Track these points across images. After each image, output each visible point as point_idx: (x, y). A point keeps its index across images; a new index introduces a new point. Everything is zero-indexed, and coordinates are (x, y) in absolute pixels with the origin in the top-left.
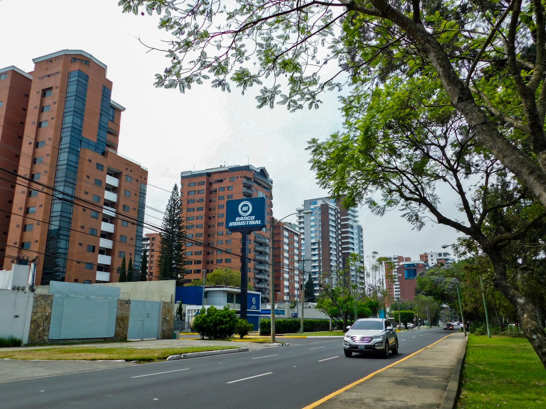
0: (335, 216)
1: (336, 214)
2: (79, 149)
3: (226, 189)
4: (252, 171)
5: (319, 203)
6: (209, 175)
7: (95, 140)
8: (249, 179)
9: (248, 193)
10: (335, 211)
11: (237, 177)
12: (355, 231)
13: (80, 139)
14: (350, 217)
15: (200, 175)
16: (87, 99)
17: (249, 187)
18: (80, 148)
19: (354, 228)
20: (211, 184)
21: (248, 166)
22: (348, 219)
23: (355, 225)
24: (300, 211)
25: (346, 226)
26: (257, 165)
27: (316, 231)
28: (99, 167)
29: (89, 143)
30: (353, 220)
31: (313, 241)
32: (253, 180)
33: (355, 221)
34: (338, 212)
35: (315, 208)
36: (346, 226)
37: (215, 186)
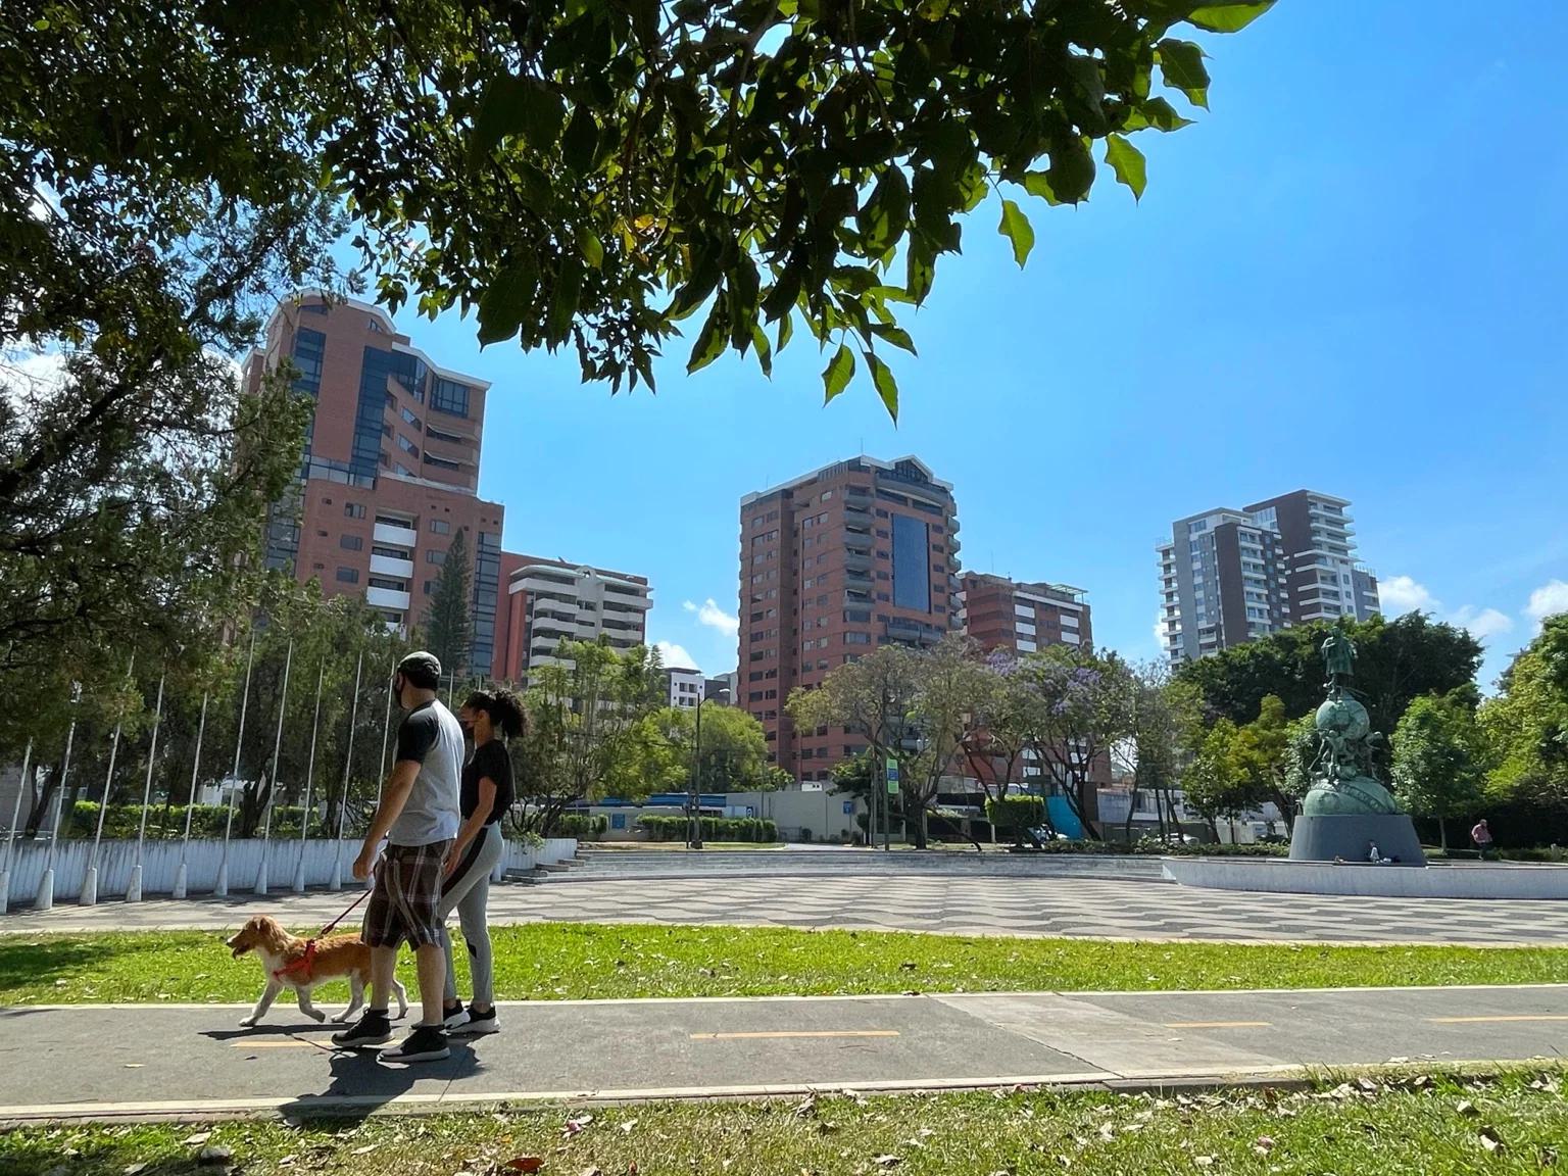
4: (866, 469)
5: (1212, 524)
6: (787, 493)
8: (863, 491)
10: (1262, 541)
12: (1345, 588)
20: (793, 513)
23: (1343, 570)
25: (1311, 577)
30: (1334, 559)
31: (1203, 624)
33: (1343, 562)
34: (1277, 543)
36: (1311, 577)
37: (798, 518)
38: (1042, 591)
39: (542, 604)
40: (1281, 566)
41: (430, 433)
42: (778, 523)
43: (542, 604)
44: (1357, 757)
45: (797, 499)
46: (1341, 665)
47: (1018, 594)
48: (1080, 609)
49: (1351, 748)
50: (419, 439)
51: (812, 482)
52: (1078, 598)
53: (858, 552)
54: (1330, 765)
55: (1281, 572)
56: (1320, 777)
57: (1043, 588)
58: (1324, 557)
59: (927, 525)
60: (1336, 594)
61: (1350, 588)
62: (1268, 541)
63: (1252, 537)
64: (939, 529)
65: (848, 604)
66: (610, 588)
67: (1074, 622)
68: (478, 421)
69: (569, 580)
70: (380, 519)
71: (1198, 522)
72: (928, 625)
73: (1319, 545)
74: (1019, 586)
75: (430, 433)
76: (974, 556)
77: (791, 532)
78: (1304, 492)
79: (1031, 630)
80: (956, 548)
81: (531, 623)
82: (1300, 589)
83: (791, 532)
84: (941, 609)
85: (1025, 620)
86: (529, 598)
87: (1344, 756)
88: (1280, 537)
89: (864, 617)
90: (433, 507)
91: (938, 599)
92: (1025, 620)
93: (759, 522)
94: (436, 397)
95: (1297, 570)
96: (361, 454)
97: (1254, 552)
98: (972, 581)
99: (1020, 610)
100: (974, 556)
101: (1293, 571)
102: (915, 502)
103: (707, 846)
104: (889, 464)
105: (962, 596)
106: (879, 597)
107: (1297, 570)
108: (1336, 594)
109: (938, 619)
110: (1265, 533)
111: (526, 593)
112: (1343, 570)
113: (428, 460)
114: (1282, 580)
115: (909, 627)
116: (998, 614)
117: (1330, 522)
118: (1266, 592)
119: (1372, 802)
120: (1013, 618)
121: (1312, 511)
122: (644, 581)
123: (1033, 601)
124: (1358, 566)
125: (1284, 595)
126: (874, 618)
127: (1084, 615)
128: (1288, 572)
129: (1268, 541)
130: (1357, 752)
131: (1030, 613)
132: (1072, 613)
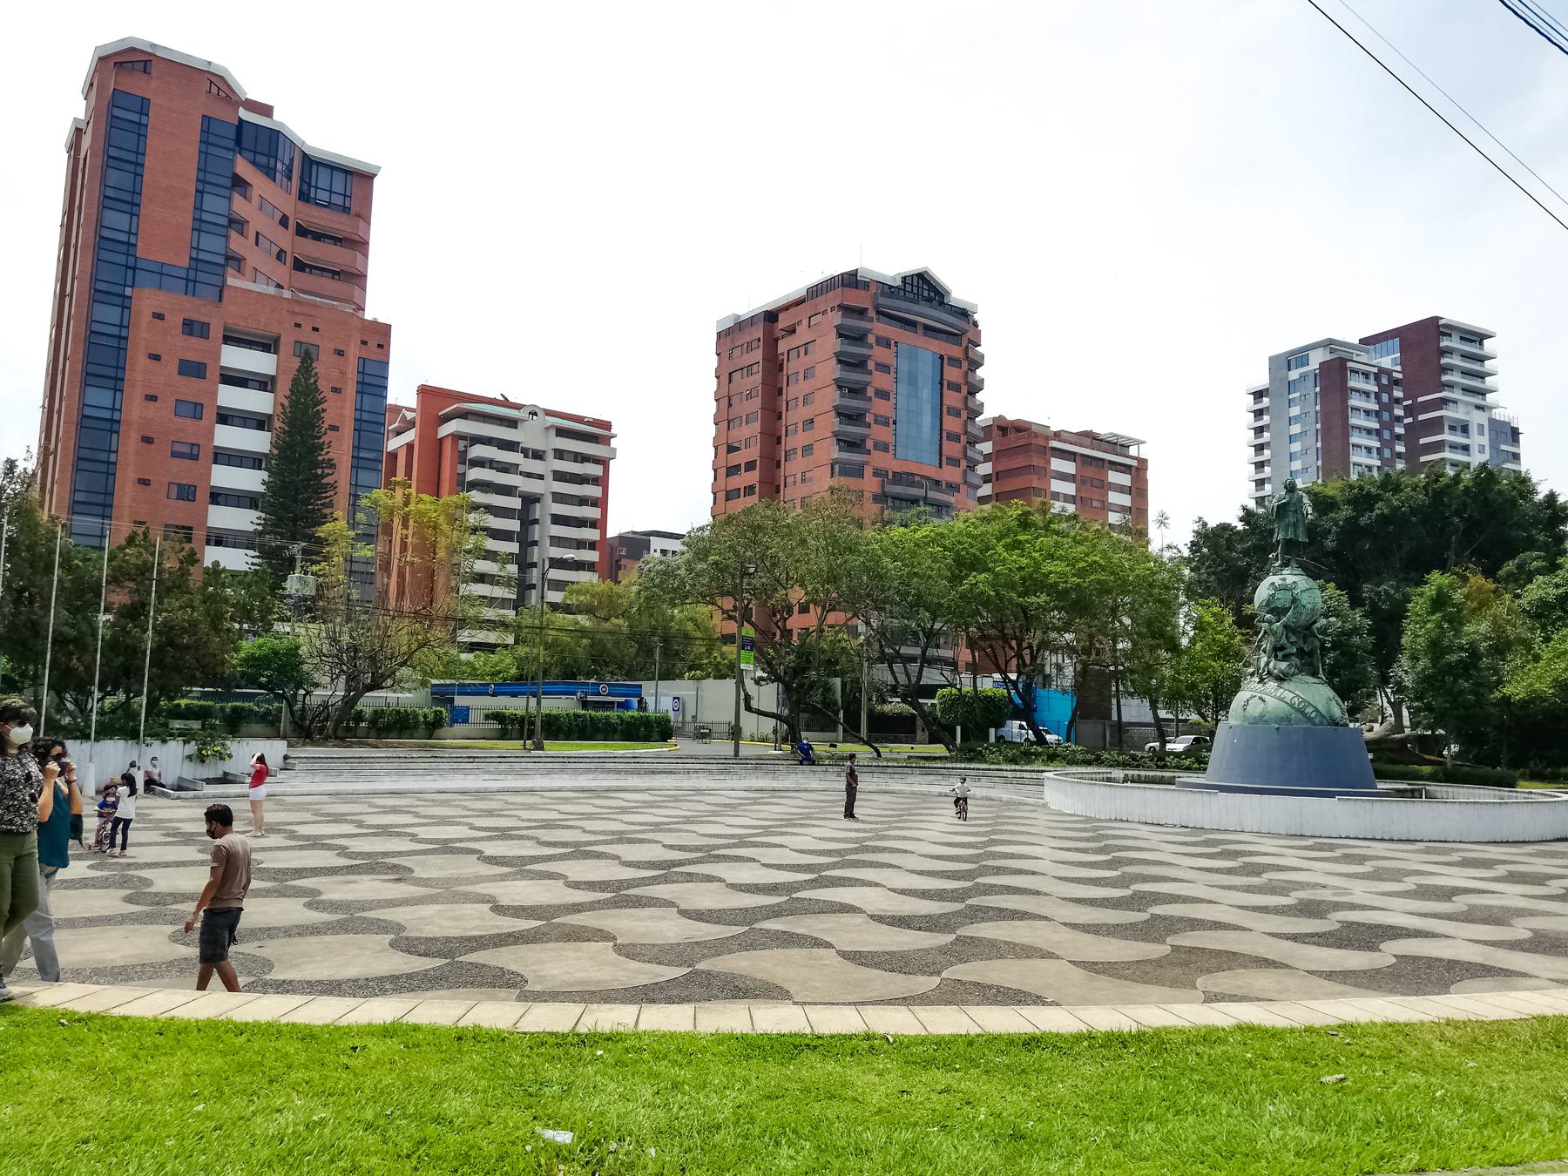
0: (1377, 396)
1: (1387, 389)
2: (128, 291)
3: (802, 350)
4: (866, 285)
5: (1316, 359)
6: (771, 316)
7: (185, 262)
8: (861, 312)
9: (851, 355)
10: (1377, 377)
11: (824, 312)
12: (1477, 440)
13: (131, 263)
14: (1456, 395)
15: (752, 320)
16: (149, 162)
17: (859, 338)
18: (132, 286)
19: (1473, 430)
20: (777, 340)
21: (854, 274)
22: (1444, 402)
23: (1477, 418)
24: (1259, 395)
26: (890, 265)
27: (1305, 451)
28: (192, 328)
29: (161, 273)
30: (1467, 404)
32: (872, 313)
33: (1478, 407)
34: (1397, 382)
35: (1303, 377)
36: (1436, 425)
37: (783, 346)
38: (1088, 441)
39: (478, 451)
40: (1399, 412)
41: (302, 231)
42: (758, 355)
43: (478, 451)
44: (1300, 650)
45: (784, 321)
46: (1291, 530)
47: (1055, 444)
48: (1134, 463)
49: (1293, 639)
50: (285, 239)
51: (799, 302)
52: (1133, 451)
53: (850, 390)
54: (1264, 659)
55: (1399, 419)
56: (1252, 675)
57: (1090, 437)
58: (1455, 402)
59: (942, 357)
60: (1466, 448)
61: (1485, 440)
62: (1384, 381)
63: (1366, 375)
64: (955, 362)
65: (836, 453)
66: (562, 432)
67: (1124, 479)
68: (364, 216)
69: (512, 423)
70: (228, 340)
71: (1298, 357)
72: (937, 483)
73: (1450, 386)
74: (1057, 435)
75: (302, 231)
76: (1004, 395)
77: (774, 365)
78: (1437, 319)
79: (1069, 488)
80: (975, 388)
81: (464, 474)
82: (1422, 441)
83: (774, 365)
84: (954, 462)
85: (1063, 477)
86: (462, 443)
87: (1282, 648)
88: (1400, 376)
89: (857, 471)
90: (298, 325)
91: (952, 449)
92: (1063, 477)
93: (737, 352)
94: (310, 186)
95: (1421, 417)
96: (202, 256)
97: (1367, 394)
98: (1004, 429)
99: (1057, 464)
100: (1004, 395)
101: (1415, 418)
102: (927, 328)
103: (553, 748)
104: (894, 278)
105: (986, 447)
106: (876, 446)
107: (1421, 417)
108: (1466, 448)
109: (951, 474)
110: (1382, 371)
111: (457, 437)
112: (1477, 418)
113: (299, 266)
114: (1399, 430)
115: (912, 484)
116: (1028, 469)
117: (1466, 356)
118: (1378, 444)
119: (1309, 710)
120: (1045, 473)
121: (1445, 343)
122: (607, 425)
123: (1074, 454)
124: (1498, 414)
125: (1400, 448)
126: (868, 471)
127: (1138, 470)
128: (1410, 420)
129: (1384, 381)
130: (1301, 644)
131: (1069, 467)
132: (1126, 469)
